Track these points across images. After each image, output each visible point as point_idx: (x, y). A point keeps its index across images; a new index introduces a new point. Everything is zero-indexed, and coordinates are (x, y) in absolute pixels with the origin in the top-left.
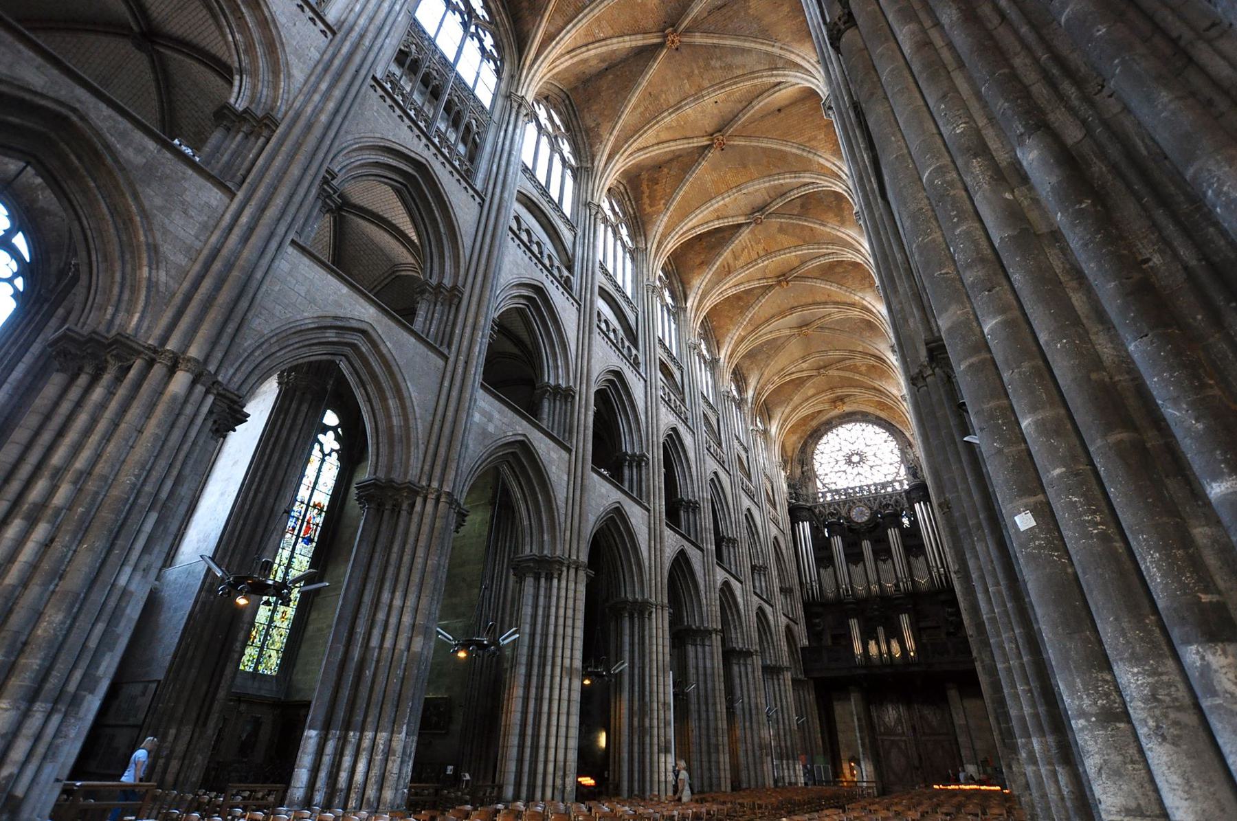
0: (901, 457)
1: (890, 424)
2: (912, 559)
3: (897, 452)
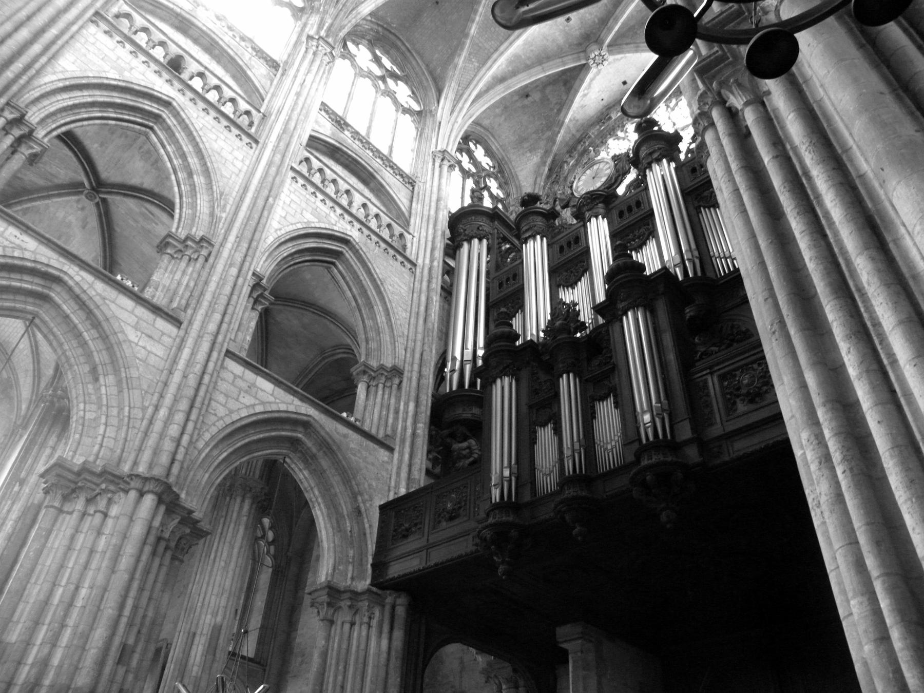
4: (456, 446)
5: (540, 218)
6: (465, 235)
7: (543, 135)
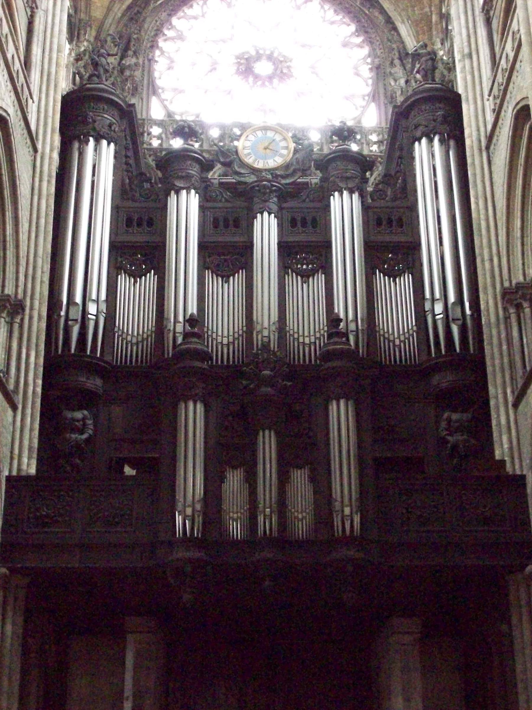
0: (376, 84)
3: (366, 71)
4: (69, 415)
5: (198, 166)
6: (94, 129)
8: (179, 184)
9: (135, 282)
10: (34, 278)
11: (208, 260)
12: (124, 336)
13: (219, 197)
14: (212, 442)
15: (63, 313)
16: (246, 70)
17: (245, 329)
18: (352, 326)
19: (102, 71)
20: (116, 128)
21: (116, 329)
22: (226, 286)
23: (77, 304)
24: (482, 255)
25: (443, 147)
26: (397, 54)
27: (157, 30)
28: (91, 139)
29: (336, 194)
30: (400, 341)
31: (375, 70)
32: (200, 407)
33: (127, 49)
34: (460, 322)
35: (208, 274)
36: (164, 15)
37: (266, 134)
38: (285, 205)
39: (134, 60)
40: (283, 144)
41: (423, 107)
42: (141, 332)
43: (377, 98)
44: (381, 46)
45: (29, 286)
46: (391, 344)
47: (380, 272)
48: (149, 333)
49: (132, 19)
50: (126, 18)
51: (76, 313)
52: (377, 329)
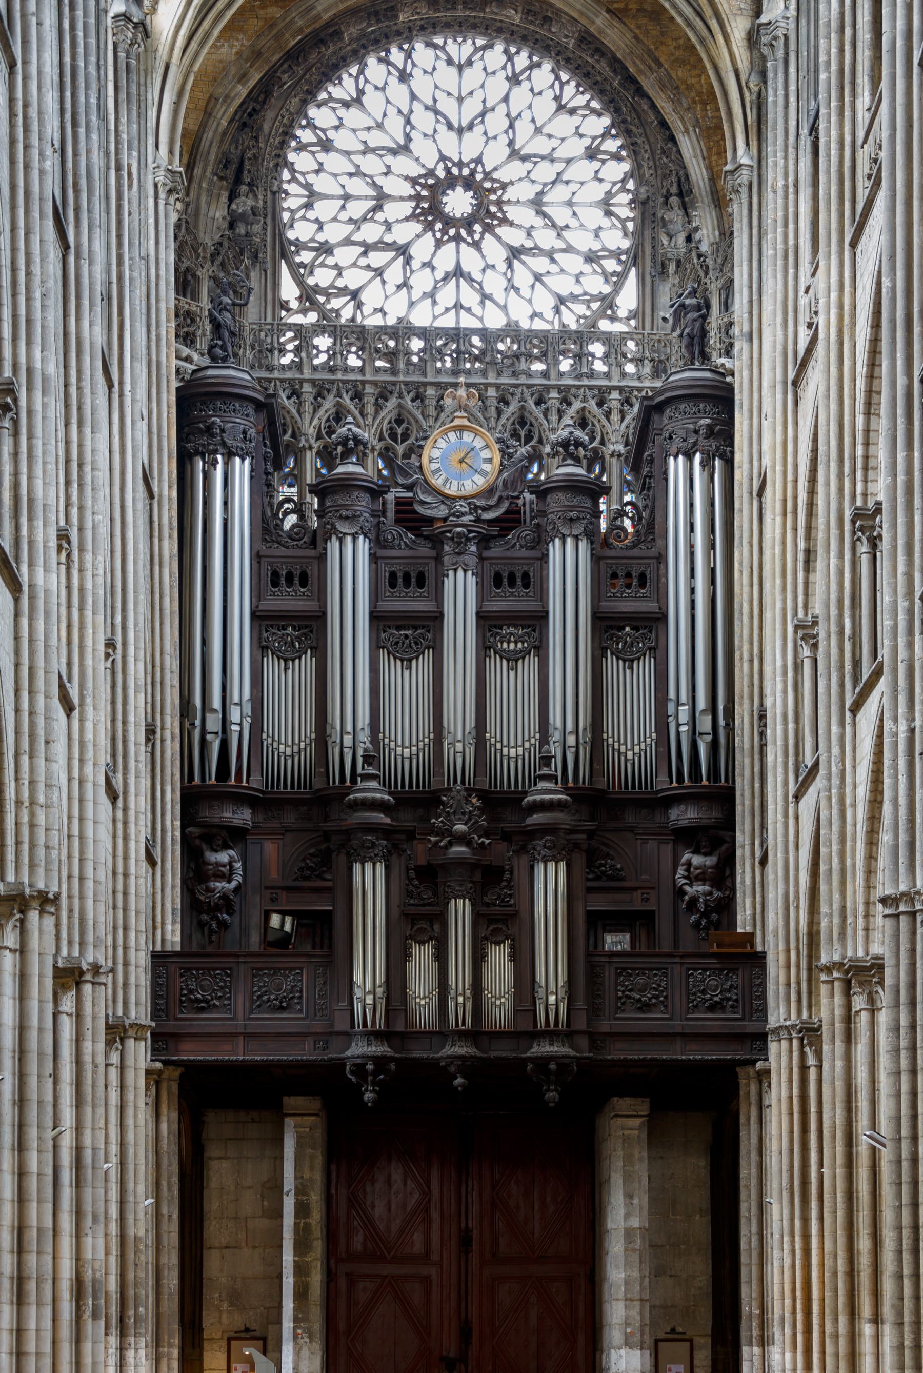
0: (638, 236)
1: (630, 80)
2: (612, 664)
6: (224, 444)
7: (263, 7)
8: (342, 527)
9: (286, 669)
10: (162, 683)
11: (383, 636)
12: (275, 745)
13: (397, 542)
14: (395, 912)
15: (198, 722)
16: (430, 208)
17: (432, 736)
18: (571, 740)
19: (226, 334)
20: (252, 432)
21: (264, 736)
22: (407, 673)
23: (216, 711)
24: (741, 648)
25: (706, 473)
26: (675, 185)
27: (285, 134)
28: (219, 457)
29: (557, 541)
30: (634, 754)
31: (639, 206)
32: (380, 868)
33: (238, 180)
34: (709, 738)
35: (383, 655)
36: (295, 101)
37: (461, 438)
38: (486, 554)
39: (250, 202)
40: (486, 454)
41: (682, 407)
42: (297, 741)
43: (639, 261)
44: (651, 163)
45: (158, 698)
46: (623, 758)
47: (612, 654)
48: (308, 741)
49: (244, 125)
50: (236, 125)
51: (213, 723)
52: (605, 736)
